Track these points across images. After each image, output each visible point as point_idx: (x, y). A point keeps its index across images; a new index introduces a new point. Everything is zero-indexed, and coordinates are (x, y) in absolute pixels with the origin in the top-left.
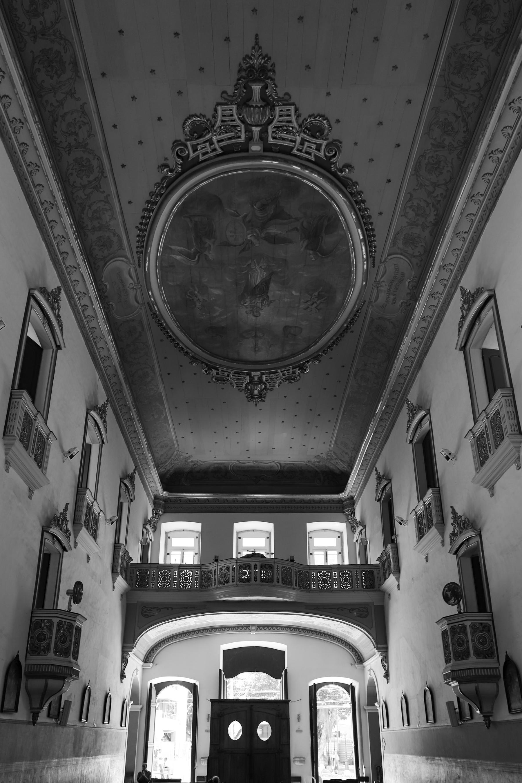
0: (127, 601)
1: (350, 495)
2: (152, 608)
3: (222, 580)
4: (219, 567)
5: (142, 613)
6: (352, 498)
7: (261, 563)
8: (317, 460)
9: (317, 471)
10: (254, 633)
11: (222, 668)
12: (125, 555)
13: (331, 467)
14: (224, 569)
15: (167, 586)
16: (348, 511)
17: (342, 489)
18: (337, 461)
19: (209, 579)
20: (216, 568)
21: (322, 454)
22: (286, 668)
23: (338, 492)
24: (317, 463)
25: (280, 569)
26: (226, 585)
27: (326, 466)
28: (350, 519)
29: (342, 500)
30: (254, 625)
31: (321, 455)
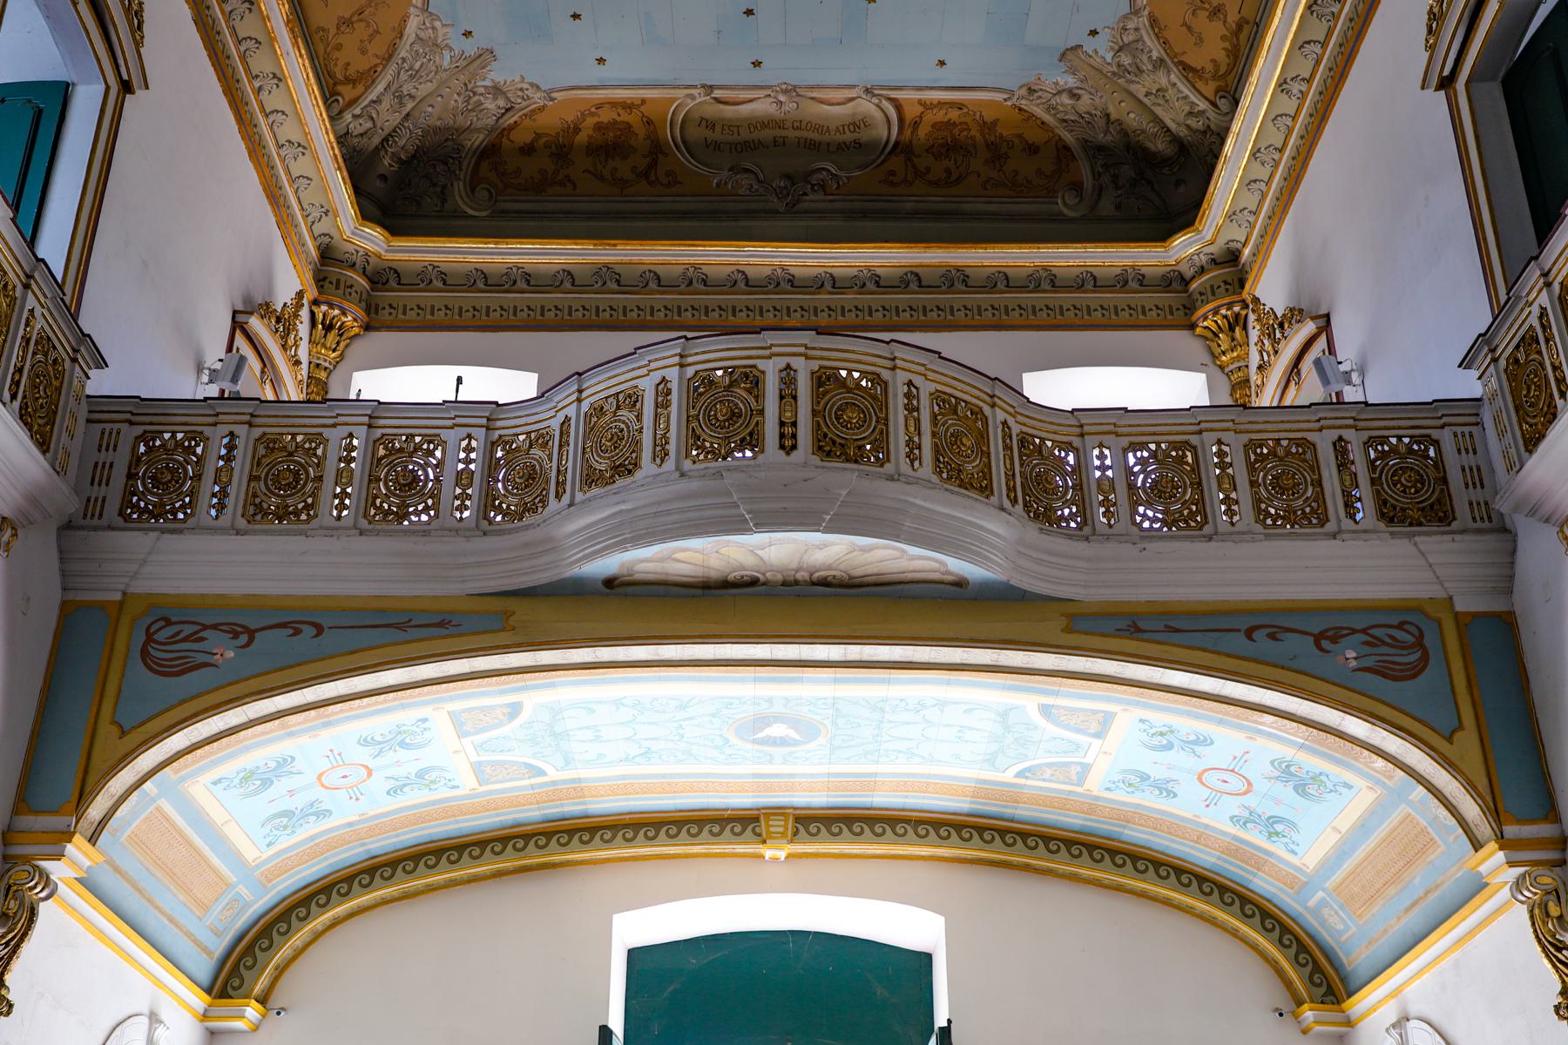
0: (64, 589)
1: (1221, 242)
2: (205, 627)
3: (602, 465)
4: (585, 406)
5: (144, 653)
6: (1231, 257)
7: (815, 365)
8: (1071, 81)
9: (1066, 148)
10: (776, 852)
11: (617, 1024)
12: (26, 286)
13: (1133, 119)
14: (610, 406)
15: (297, 513)
16: (1216, 312)
17: (1184, 215)
18: (1164, 81)
19: (532, 476)
20: (571, 411)
21: (1094, 33)
22: (940, 1021)
23: (1163, 234)
24: (1066, 99)
25: (925, 402)
26: (620, 482)
27: (1108, 115)
28: (1224, 353)
29: (1182, 278)
30: (778, 811)
31: (1090, 45)
